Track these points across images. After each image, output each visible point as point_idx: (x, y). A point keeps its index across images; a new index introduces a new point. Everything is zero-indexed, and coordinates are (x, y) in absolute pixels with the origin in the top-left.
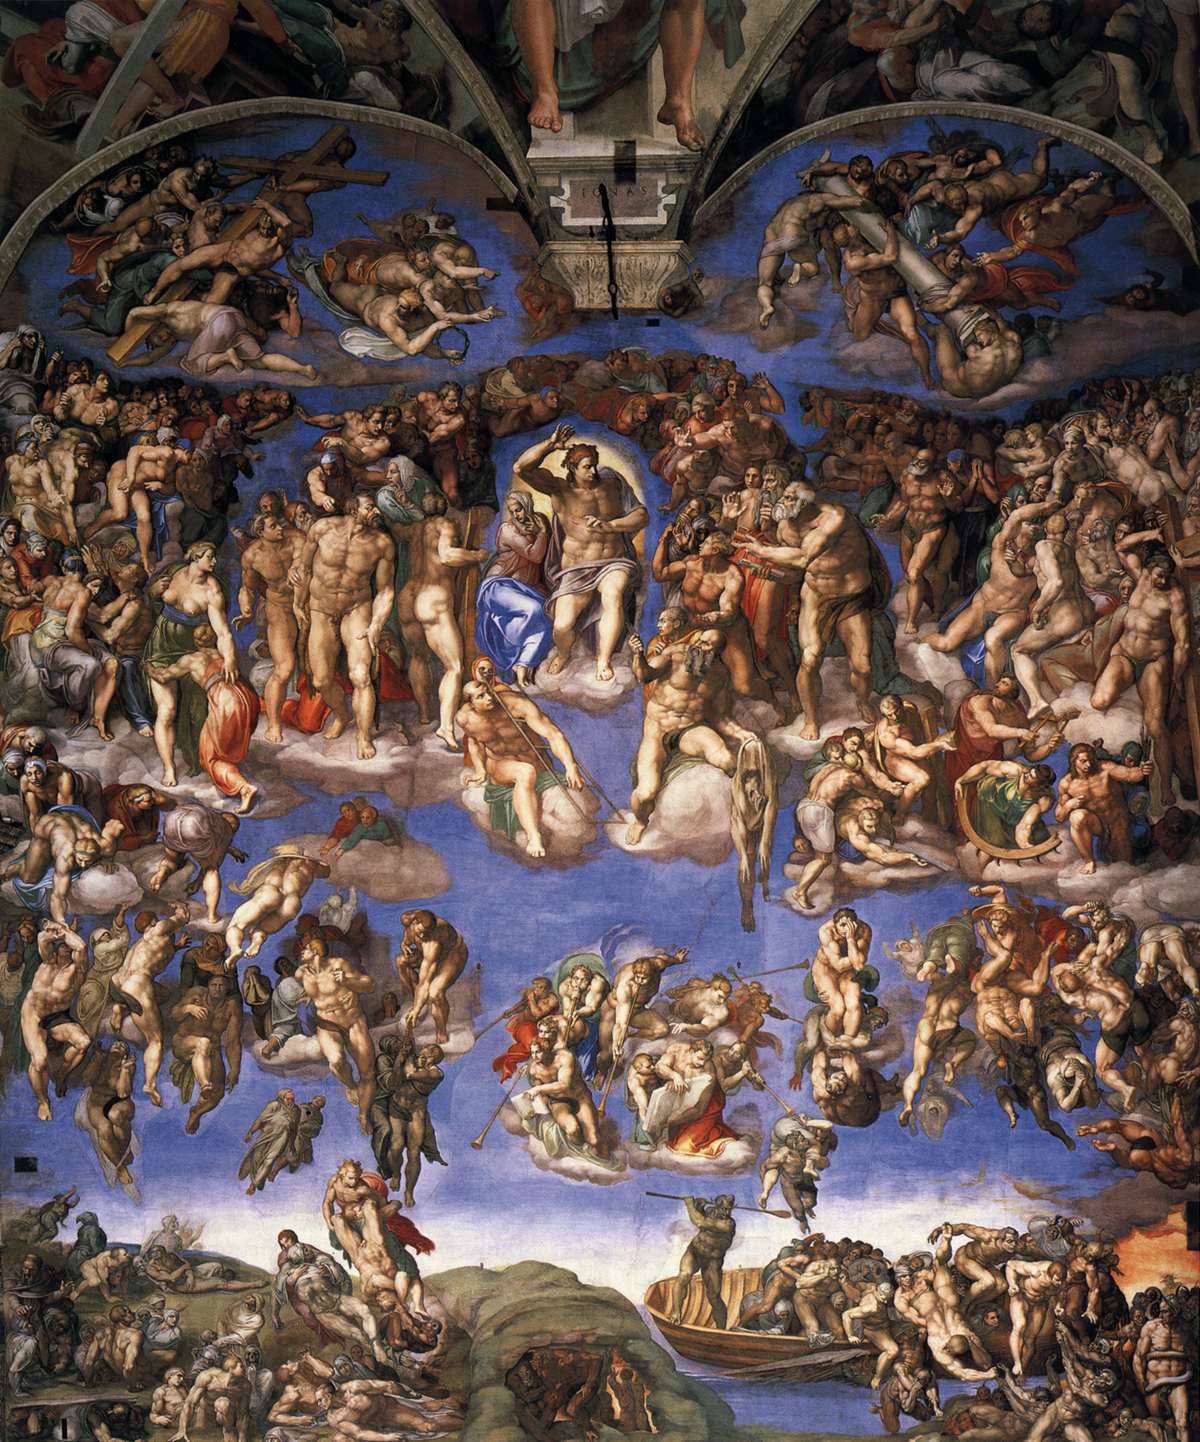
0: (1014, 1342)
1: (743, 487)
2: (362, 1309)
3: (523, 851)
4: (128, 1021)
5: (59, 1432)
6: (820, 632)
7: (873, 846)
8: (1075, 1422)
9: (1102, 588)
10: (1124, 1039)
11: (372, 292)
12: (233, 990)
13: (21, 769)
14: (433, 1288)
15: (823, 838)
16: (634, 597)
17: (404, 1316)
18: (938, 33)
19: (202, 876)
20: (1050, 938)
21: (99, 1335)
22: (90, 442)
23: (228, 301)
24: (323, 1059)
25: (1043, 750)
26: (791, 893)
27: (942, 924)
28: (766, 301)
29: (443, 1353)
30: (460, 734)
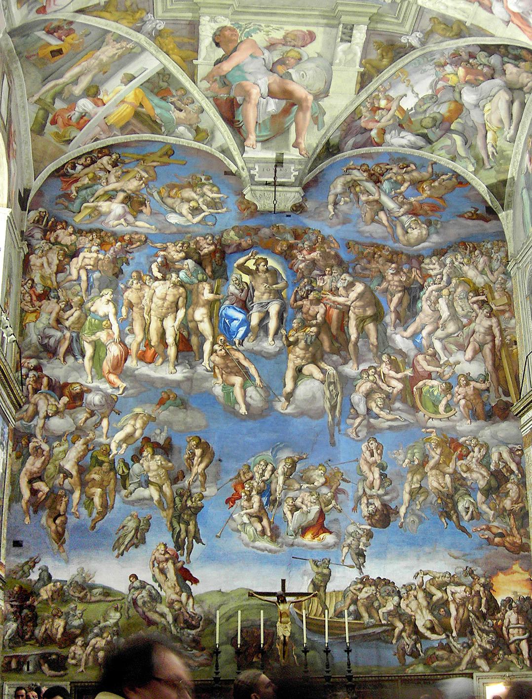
0: (452, 622)
1: (325, 275)
2: (166, 610)
3: (238, 412)
4: (66, 481)
5: (25, 667)
6: (357, 329)
7: (382, 412)
8: (480, 657)
9: (465, 316)
10: (488, 492)
11: (179, 201)
12: (113, 468)
13: (27, 376)
14: (198, 601)
15: (362, 409)
16: (283, 314)
17: (185, 613)
18: (393, 124)
19: (101, 420)
20: (455, 450)
21: (46, 621)
22: (64, 251)
23: (122, 202)
24: (151, 499)
25: (447, 376)
26: (350, 431)
27: (411, 444)
28: (331, 210)
29: (203, 630)
30: (212, 365)
